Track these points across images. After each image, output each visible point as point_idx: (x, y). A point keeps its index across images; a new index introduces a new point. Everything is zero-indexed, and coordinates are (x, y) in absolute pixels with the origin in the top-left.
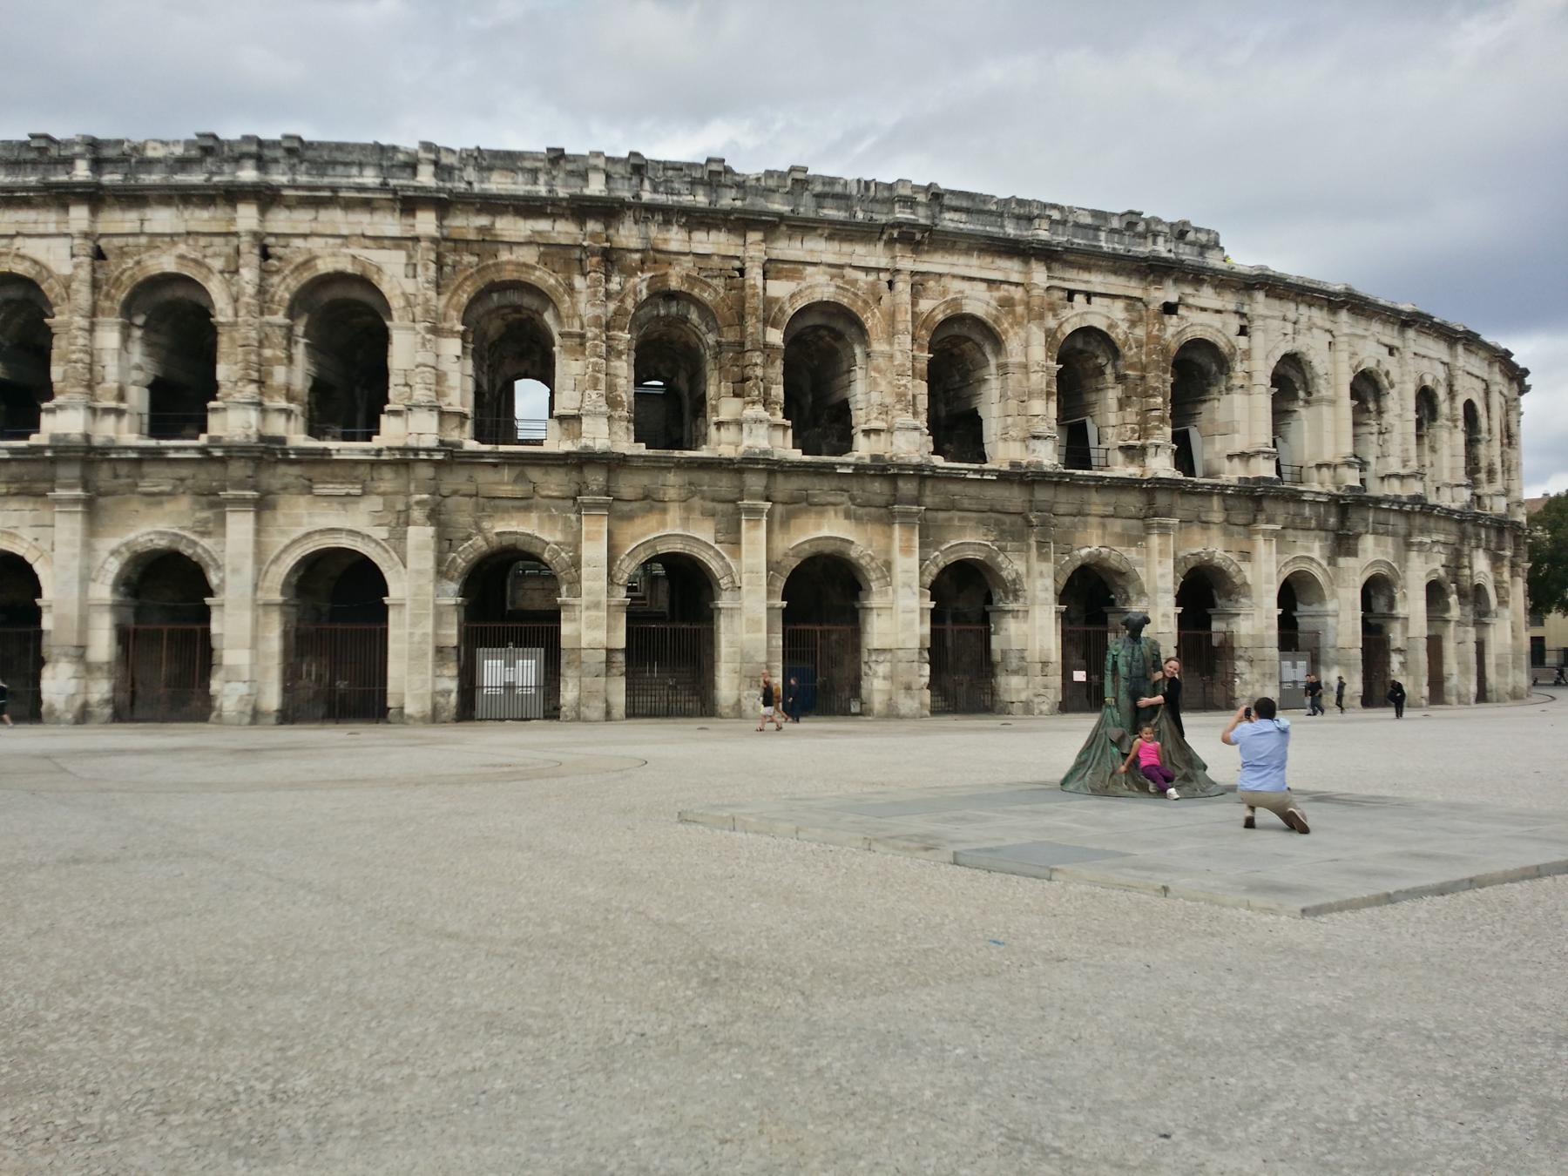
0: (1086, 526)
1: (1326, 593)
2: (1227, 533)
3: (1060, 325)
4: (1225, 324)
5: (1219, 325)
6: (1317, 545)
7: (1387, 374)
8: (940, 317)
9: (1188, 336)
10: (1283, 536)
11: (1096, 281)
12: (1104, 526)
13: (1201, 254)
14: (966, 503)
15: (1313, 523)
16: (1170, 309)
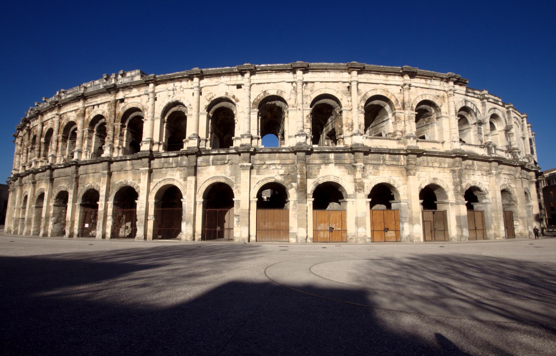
0: (89, 177)
1: (182, 192)
2: (134, 173)
3: (89, 117)
4: (142, 100)
5: (139, 101)
6: (178, 173)
7: (234, 97)
8: (65, 124)
9: (127, 108)
10: (161, 171)
11: (99, 100)
12: (94, 176)
13: (132, 79)
14: (62, 175)
15: (174, 165)
16: (122, 101)
